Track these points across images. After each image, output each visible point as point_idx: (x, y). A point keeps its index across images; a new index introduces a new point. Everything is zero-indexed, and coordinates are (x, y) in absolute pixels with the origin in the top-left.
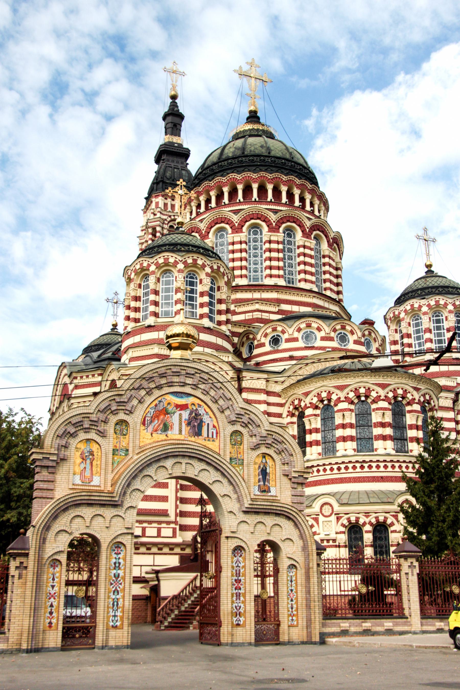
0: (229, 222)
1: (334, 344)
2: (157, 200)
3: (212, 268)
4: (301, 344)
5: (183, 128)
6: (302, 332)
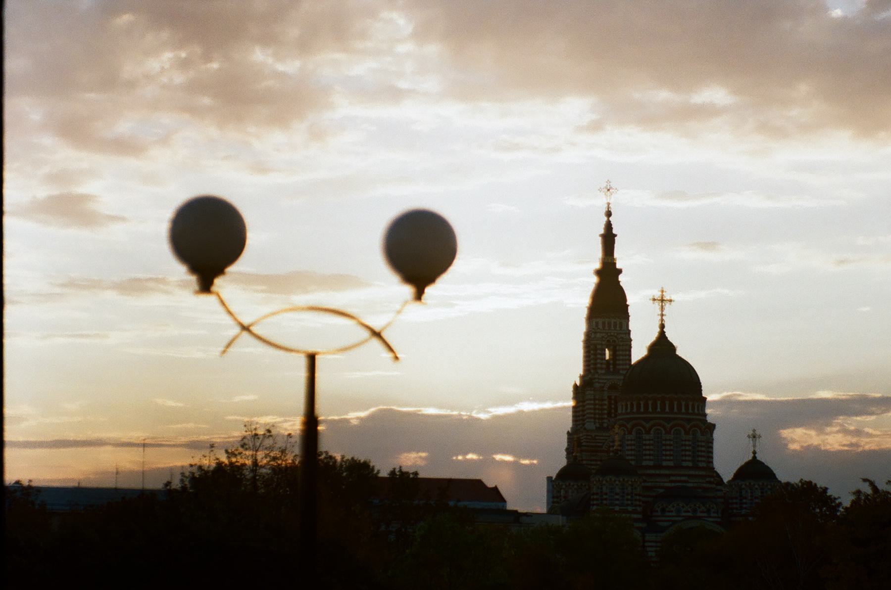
0: (644, 427)
1: (690, 514)
2: (598, 320)
3: (631, 481)
4: (674, 514)
5: (615, 245)
6: (675, 508)
